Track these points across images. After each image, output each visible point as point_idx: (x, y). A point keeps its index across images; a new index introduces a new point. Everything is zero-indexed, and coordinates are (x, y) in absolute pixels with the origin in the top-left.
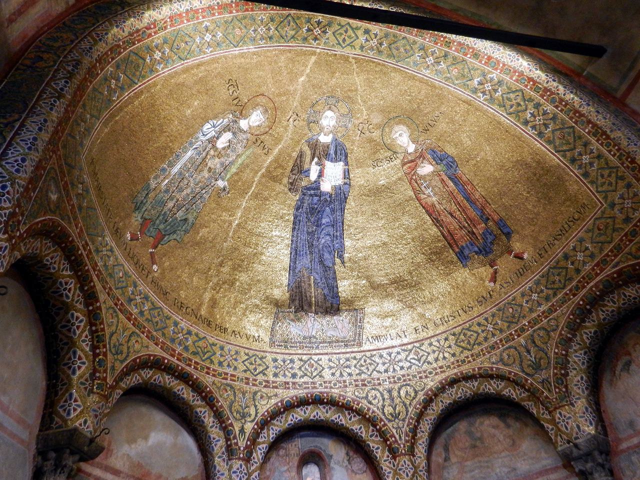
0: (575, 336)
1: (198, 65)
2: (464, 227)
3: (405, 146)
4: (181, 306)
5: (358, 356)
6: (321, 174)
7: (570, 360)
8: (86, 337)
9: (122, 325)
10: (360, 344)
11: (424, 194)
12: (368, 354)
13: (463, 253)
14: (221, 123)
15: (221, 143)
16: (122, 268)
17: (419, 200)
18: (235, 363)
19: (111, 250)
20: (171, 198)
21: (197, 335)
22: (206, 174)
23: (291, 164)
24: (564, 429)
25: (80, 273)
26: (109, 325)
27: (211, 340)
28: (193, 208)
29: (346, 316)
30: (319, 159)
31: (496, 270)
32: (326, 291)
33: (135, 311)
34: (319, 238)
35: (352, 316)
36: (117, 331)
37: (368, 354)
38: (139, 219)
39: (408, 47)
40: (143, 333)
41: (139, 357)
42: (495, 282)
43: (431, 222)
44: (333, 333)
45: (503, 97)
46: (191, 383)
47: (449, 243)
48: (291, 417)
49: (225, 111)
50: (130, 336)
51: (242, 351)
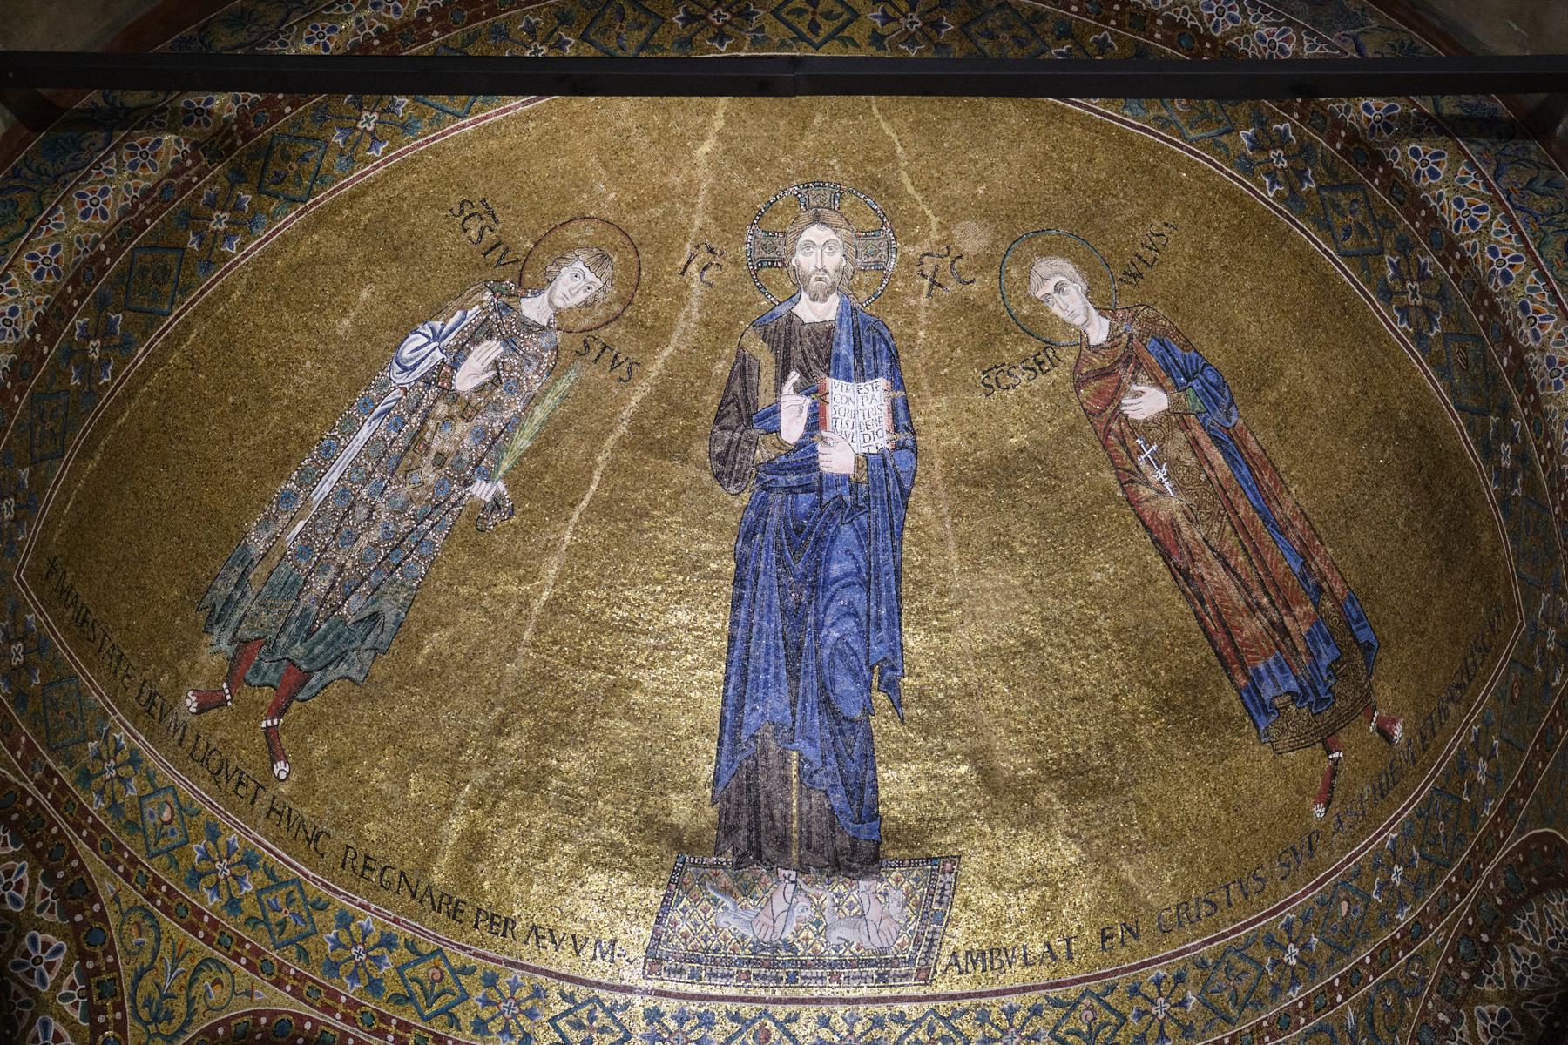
0: (1456, 1020)
1: (353, 197)
2: (1258, 604)
3: (1079, 321)
4: (366, 867)
5: (912, 1011)
6: (816, 422)
8: (73, 986)
9: (169, 946)
10: (926, 977)
11: (1148, 484)
12: (943, 1007)
13: (1258, 692)
14: (459, 324)
15: (467, 379)
16: (171, 799)
17: (1132, 502)
18: (526, 1023)
19: (134, 760)
20: (319, 566)
21: (411, 946)
22: (430, 475)
23: (712, 399)
25: (39, 845)
26: (129, 953)
27: (458, 959)
29: (897, 881)
30: (806, 373)
31: (1336, 762)
32: (838, 799)
33: (210, 902)
34: (819, 626)
35: (917, 879)
36: (156, 964)
37: (943, 1007)
38: (224, 645)
39: (1023, 33)
40: (236, 957)
41: (225, 1022)
42: (1327, 805)
43: (1169, 577)
44: (846, 933)
45: (1322, 199)
47: (1219, 656)
49: (463, 287)
50: (197, 970)
51: (554, 989)
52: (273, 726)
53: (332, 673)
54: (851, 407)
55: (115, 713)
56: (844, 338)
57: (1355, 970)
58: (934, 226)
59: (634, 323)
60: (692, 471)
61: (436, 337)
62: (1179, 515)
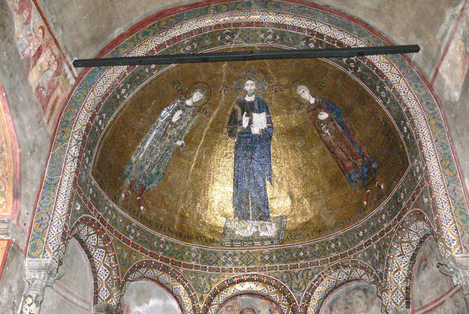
2: (350, 159)
3: (308, 99)
4: (161, 227)
7: (395, 261)
8: (107, 259)
11: (324, 133)
13: (350, 177)
14: (172, 107)
15: (174, 119)
17: (321, 137)
20: (147, 163)
22: (168, 140)
23: (228, 119)
24: (384, 303)
30: (248, 112)
42: (367, 201)
46: (170, 272)
48: (234, 289)
53: (151, 186)
54: (258, 119)
56: (256, 104)
57: (375, 236)
58: (275, 79)
59: (210, 104)
60: (224, 135)
61: (168, 110)
62: (332, 140)
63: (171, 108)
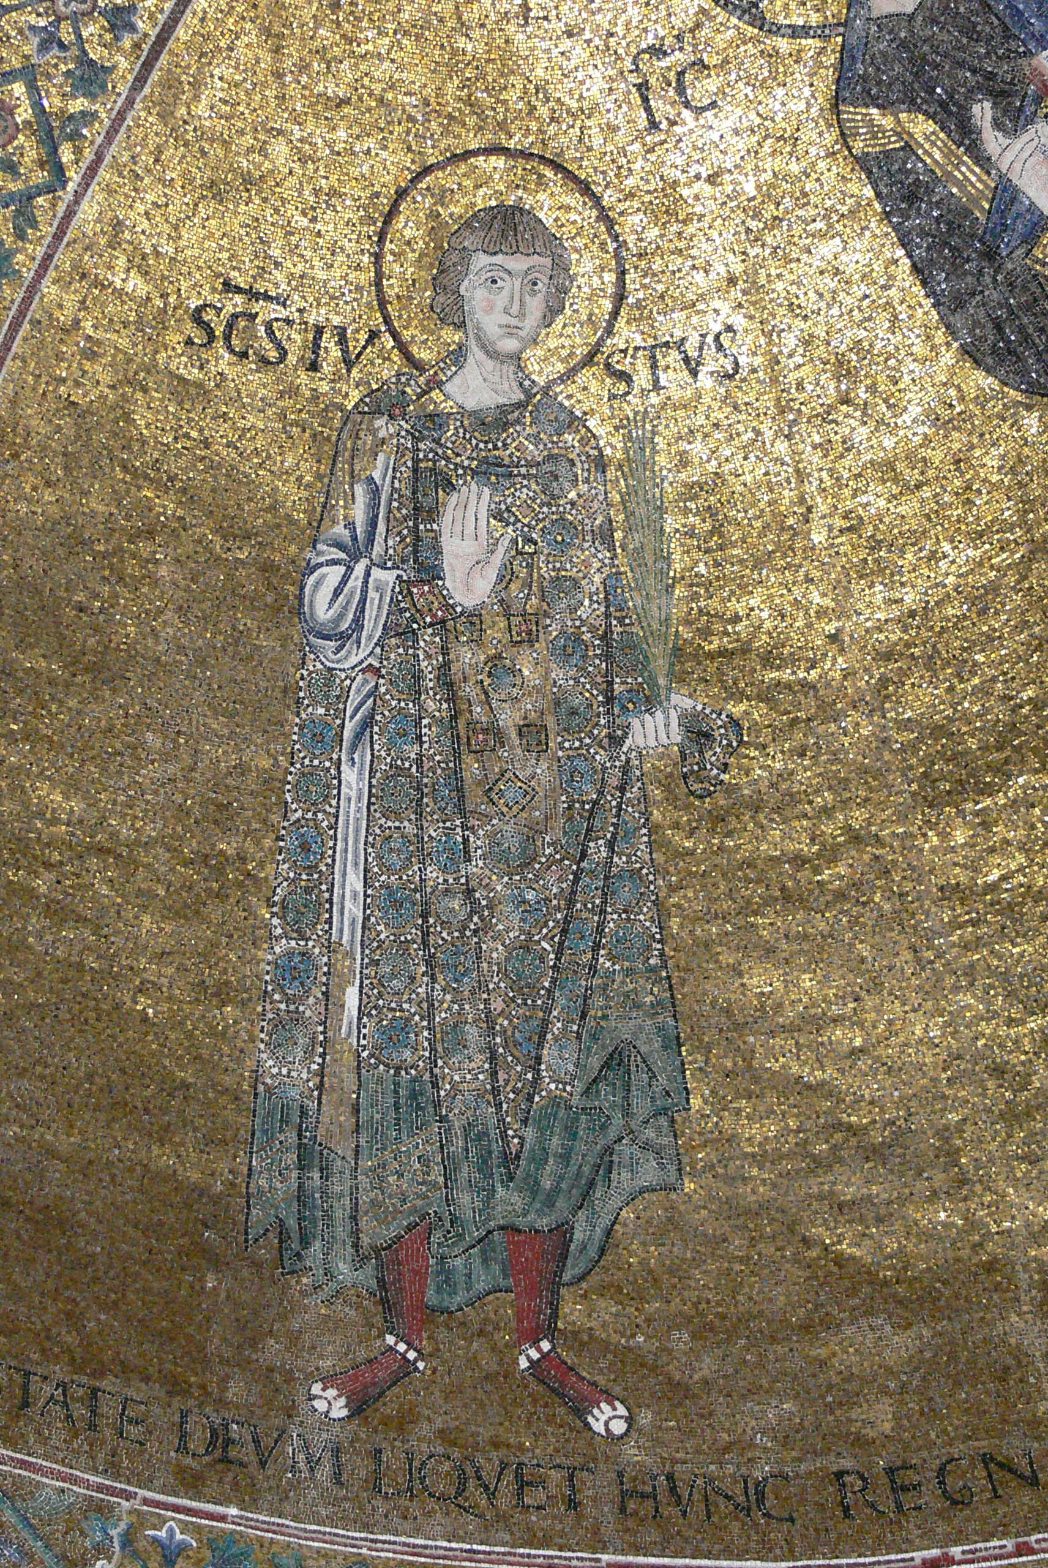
28: (610, 975)
38: (343, 1269)
52: (545, 1356)
55: (129, 1496)
61: (354, 551)
63: (359, 513)
